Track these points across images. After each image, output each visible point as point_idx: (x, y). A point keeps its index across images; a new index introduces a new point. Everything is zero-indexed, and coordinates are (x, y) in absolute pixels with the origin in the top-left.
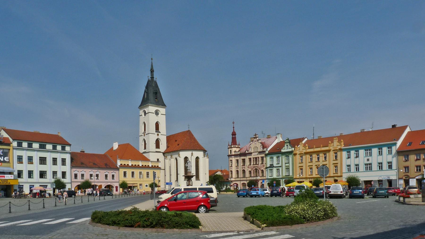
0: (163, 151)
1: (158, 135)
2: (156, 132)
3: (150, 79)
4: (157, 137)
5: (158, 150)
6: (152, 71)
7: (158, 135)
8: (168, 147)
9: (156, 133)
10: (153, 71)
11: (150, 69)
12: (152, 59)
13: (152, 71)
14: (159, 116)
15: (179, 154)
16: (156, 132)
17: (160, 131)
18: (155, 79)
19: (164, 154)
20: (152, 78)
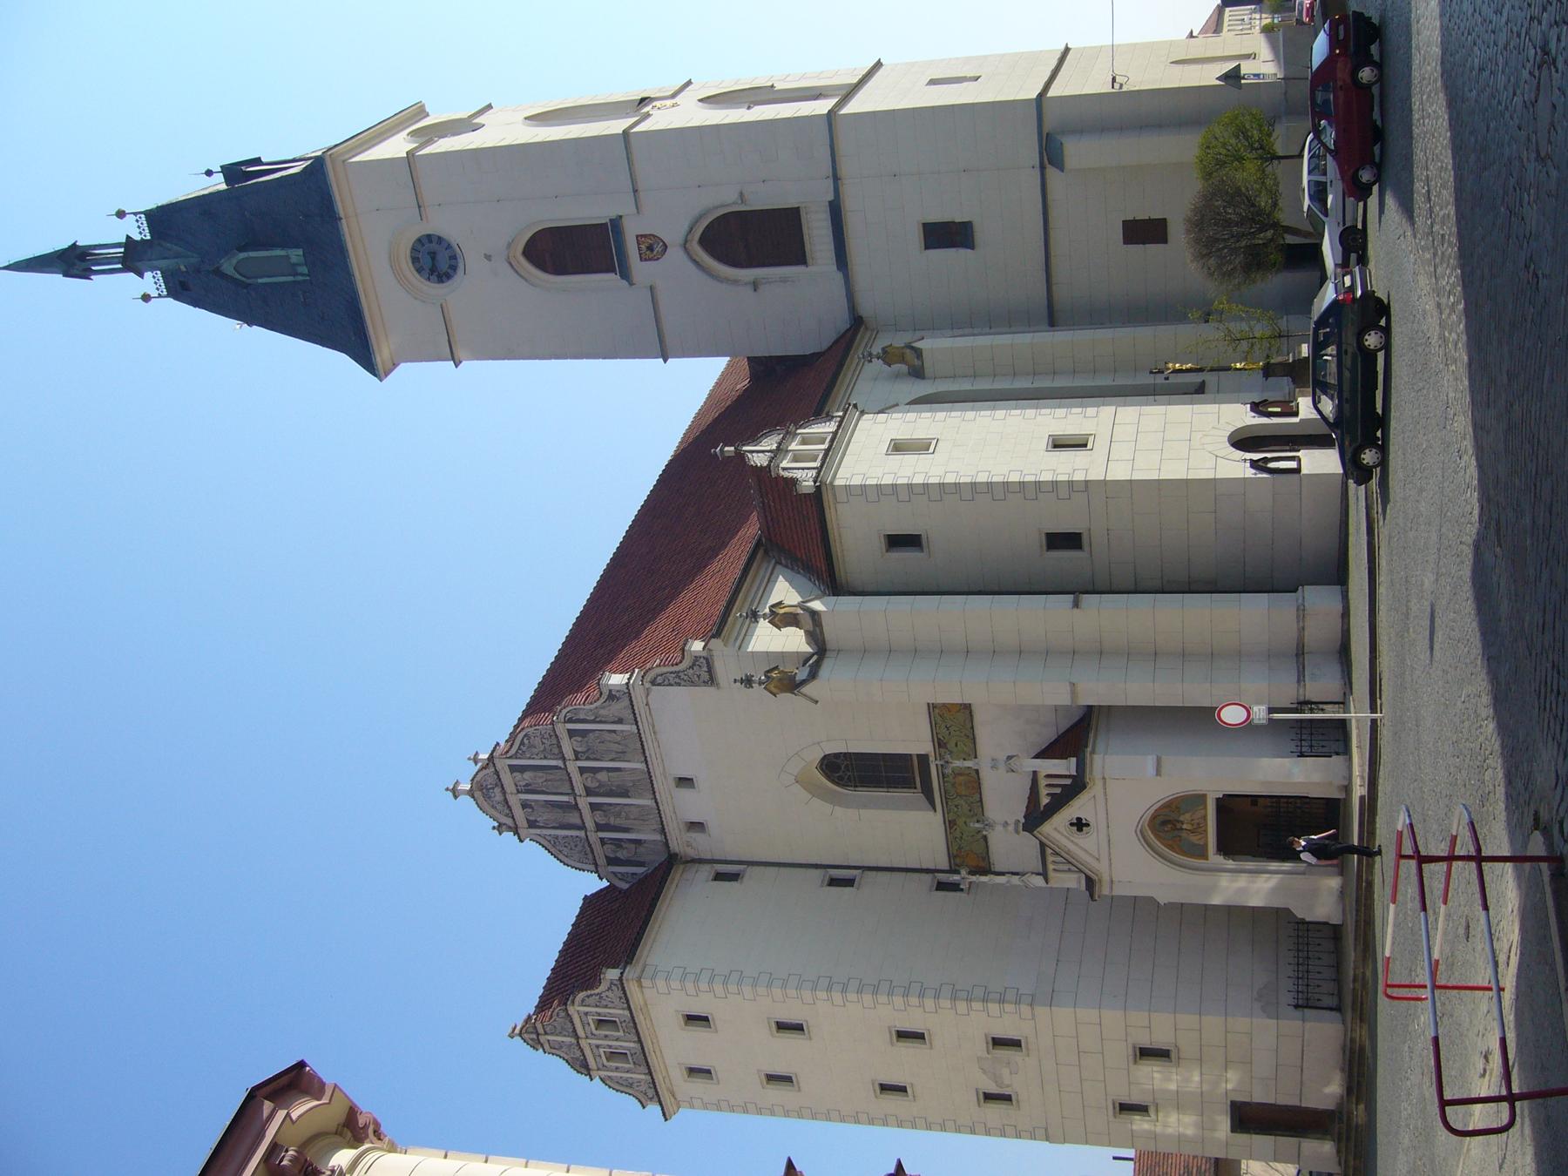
3: (150, 282)
6: (75, 262)
13: (75, 262)
18: (136, 230)
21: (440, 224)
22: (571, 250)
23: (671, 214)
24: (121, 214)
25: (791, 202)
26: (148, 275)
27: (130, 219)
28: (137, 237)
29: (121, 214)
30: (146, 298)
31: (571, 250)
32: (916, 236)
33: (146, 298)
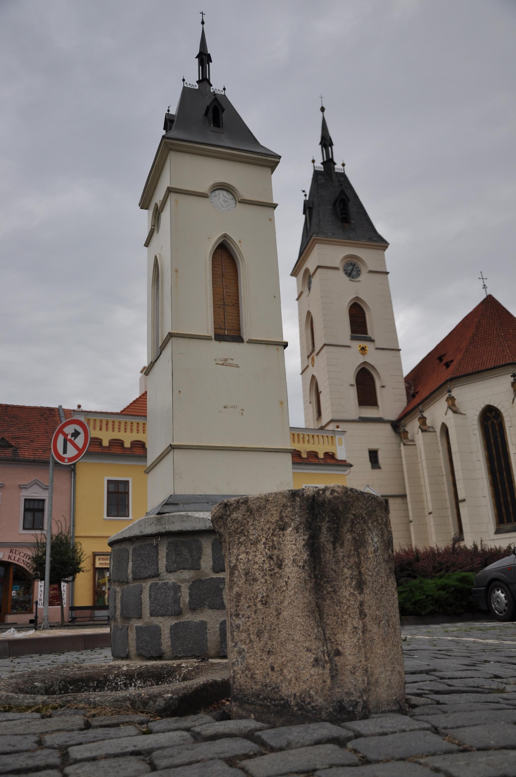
0: (393, 416)
1: (363, 349)
2: (353, 338)
4: (360, 359)
5: (369, 412)
6: (326, 142)
7: (363, 349)
8: (411, 395)
9: (357, 345)
10: (331, 144)
11: (319, 140)
12: (323, 109)
13: (326, 142)
14: (361, 278)
15: (451, 399)
16: (353, 338)
17: (370, 334)
18: (338, 167)
19: (397, 426)
20: (329, 163)
21: (364, 276)
22: (358, 319)
23: (373, 357)
24: (343, 165)
25: (379, 403)
26: (322, 166)
27: (342, 168)
28: (336, 166)
29: (343, 165)
30: (313, 161)
31: (358, 319)
32: (374, 447)
33: (313, 161)
